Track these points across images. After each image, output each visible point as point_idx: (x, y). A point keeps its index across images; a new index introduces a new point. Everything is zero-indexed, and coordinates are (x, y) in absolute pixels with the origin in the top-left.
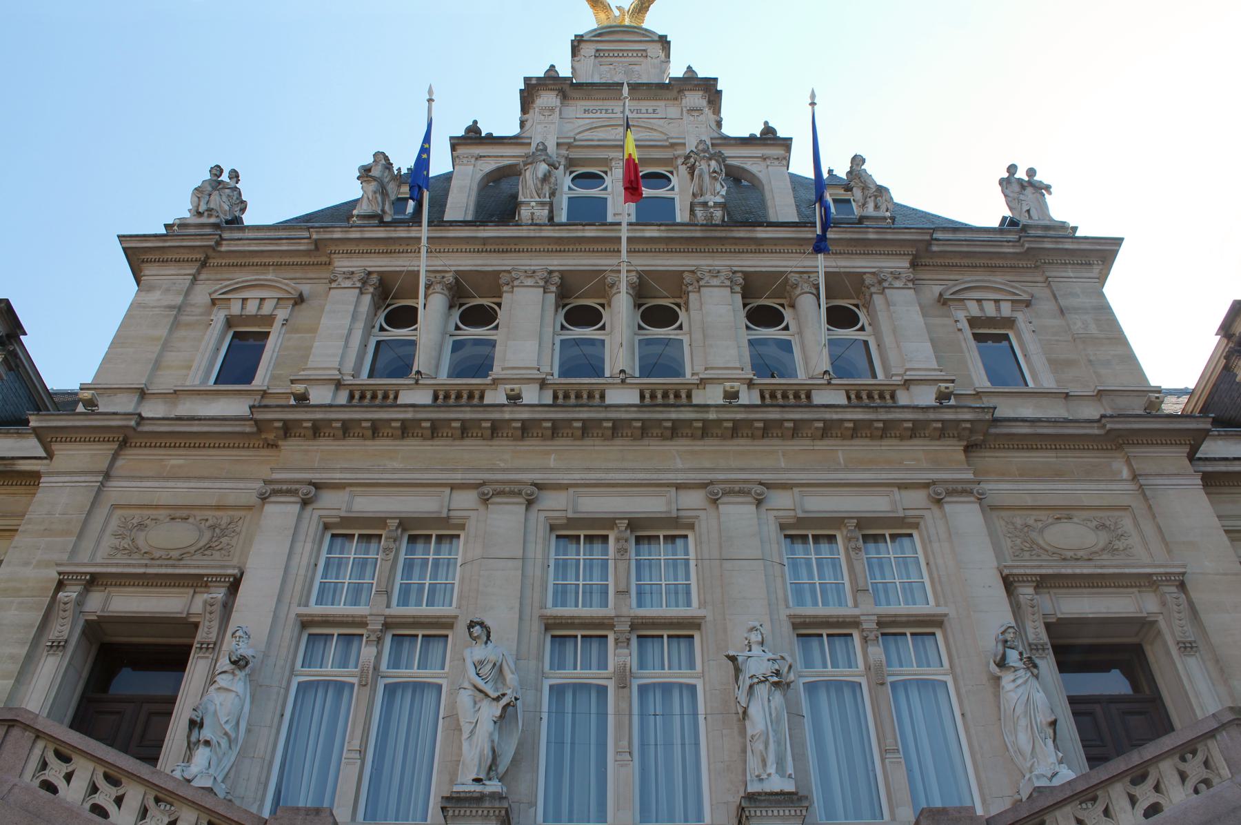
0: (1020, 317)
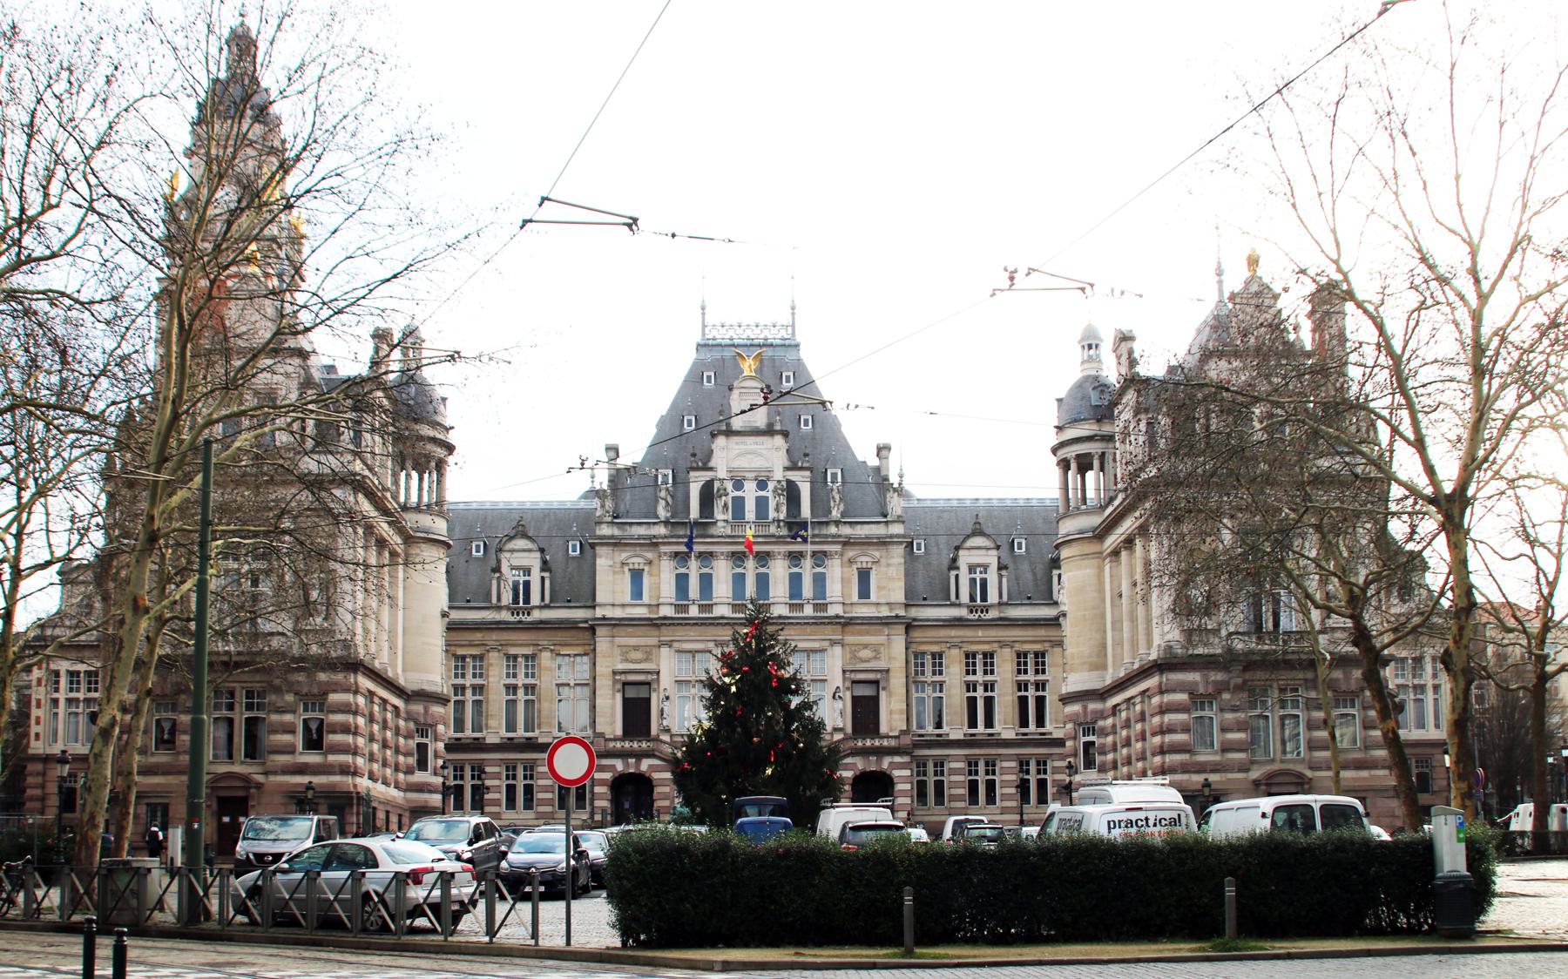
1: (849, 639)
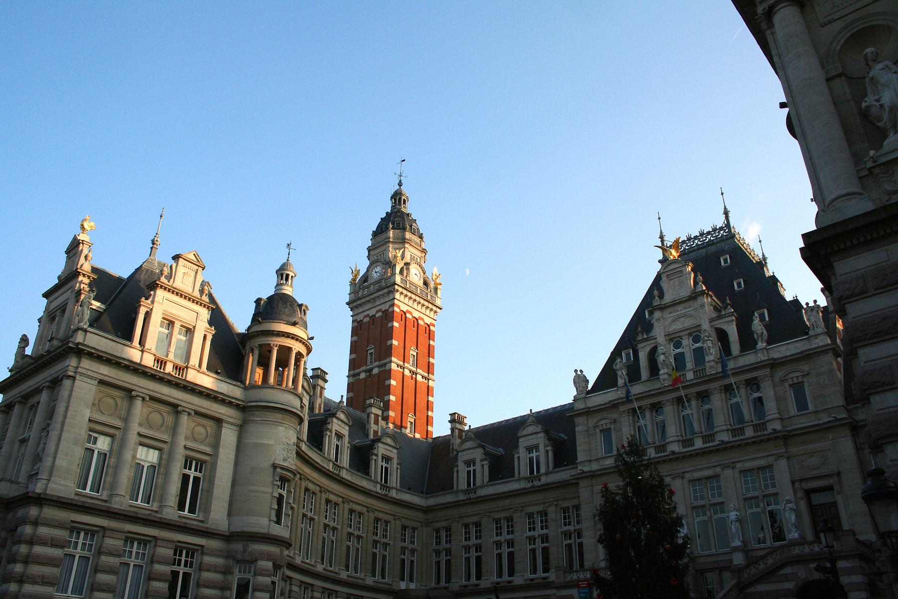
0: (805, 380)
1: (794, 450)
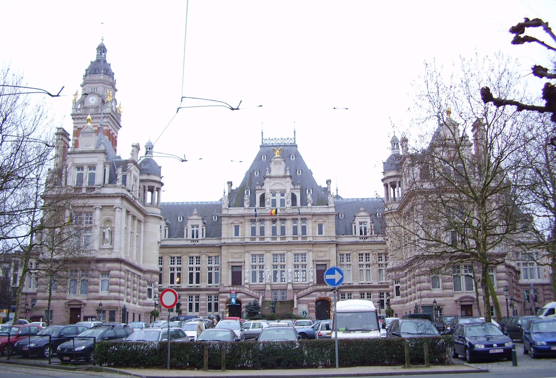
1: (315, 249)
